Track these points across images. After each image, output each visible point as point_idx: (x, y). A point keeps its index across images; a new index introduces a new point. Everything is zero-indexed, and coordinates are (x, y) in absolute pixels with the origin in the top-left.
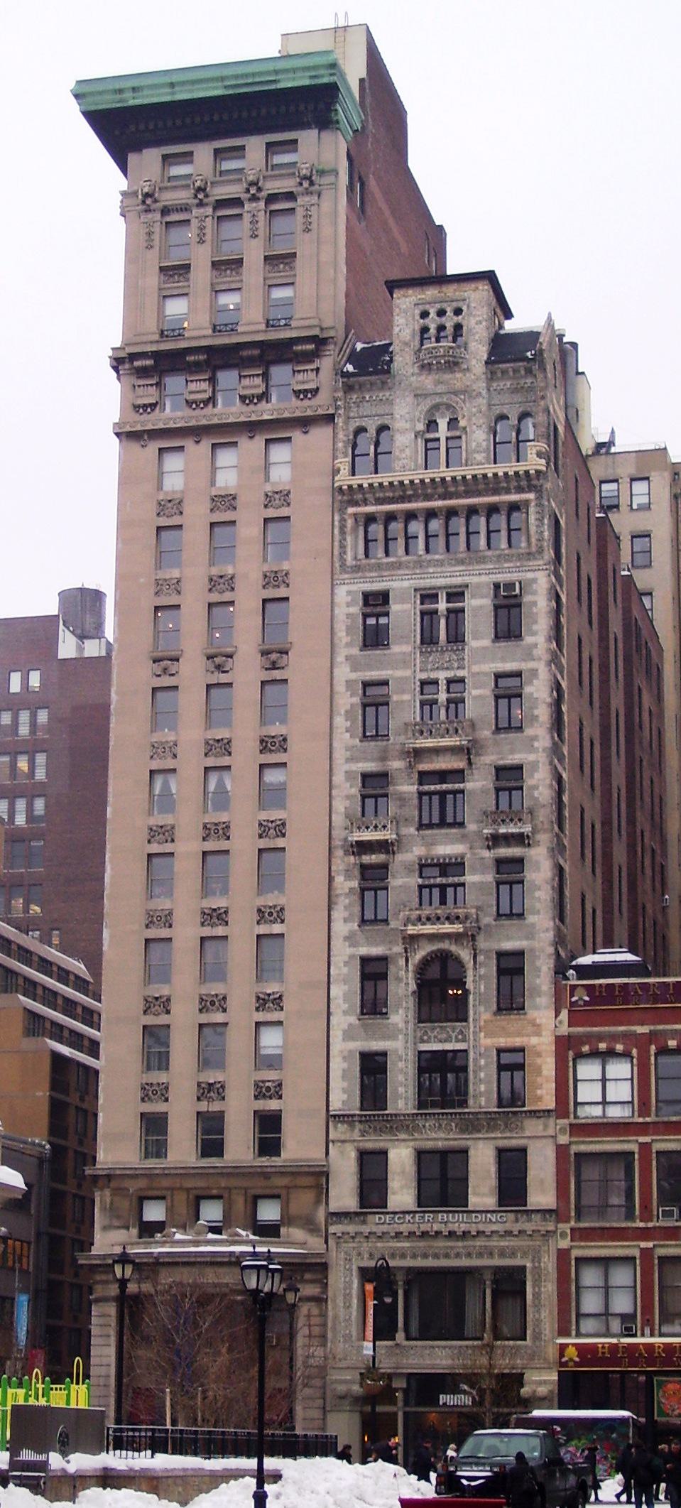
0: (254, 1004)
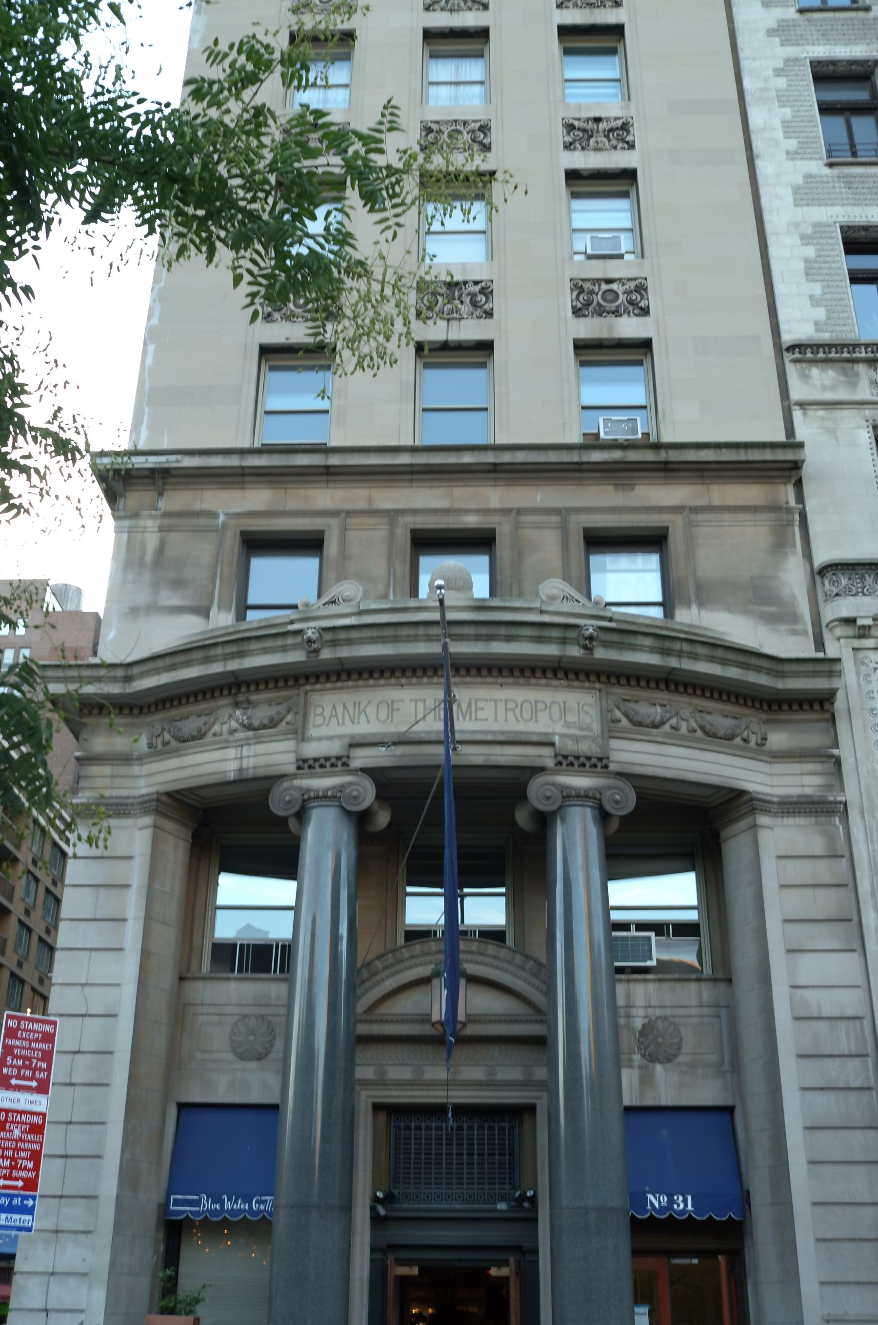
0: (559, 134)
